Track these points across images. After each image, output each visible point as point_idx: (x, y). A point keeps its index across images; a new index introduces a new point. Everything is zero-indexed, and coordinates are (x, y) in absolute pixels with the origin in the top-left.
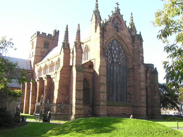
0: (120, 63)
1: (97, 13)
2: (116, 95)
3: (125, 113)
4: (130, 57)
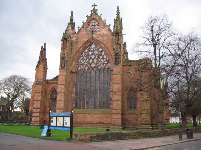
0: (99, 67)
1: (72, 24)
2: (93, 102)
3: (102, 121)
4: (111, 57)
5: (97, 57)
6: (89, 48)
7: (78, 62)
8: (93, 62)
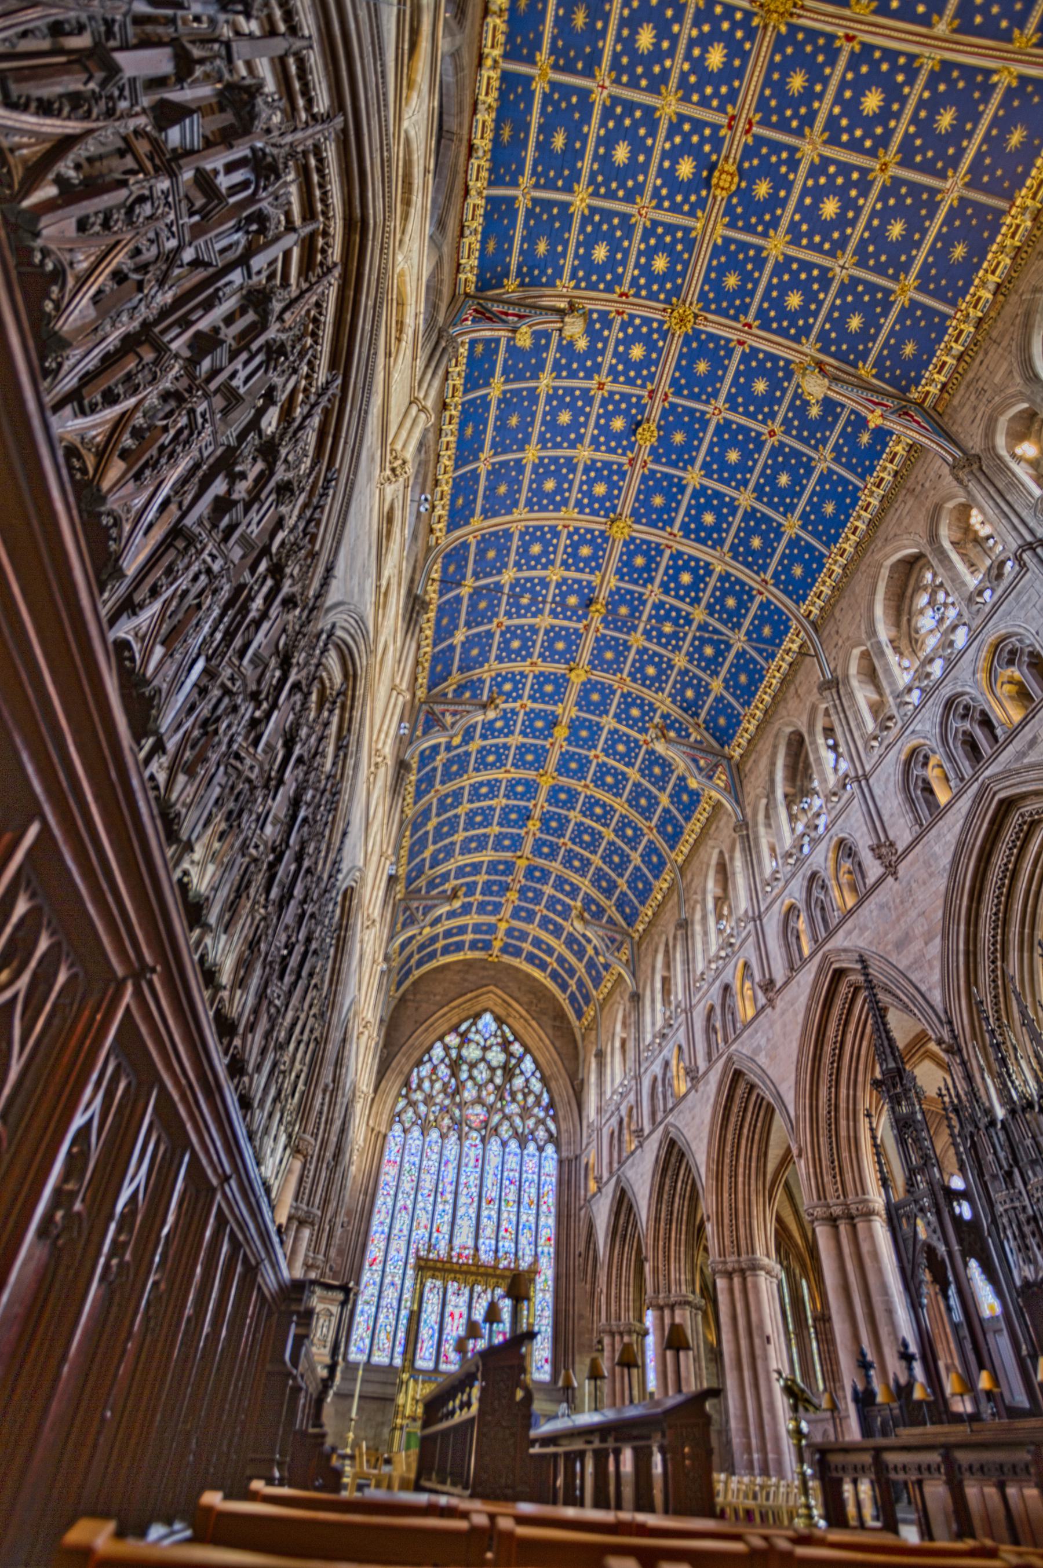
5: (498, 1081)
6: (468, 1030)
7: (407, 1084)
8: (479, 1100)
